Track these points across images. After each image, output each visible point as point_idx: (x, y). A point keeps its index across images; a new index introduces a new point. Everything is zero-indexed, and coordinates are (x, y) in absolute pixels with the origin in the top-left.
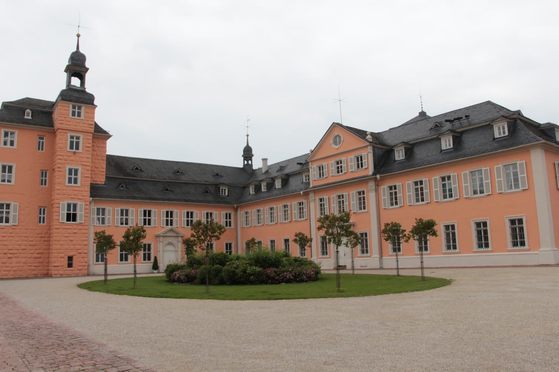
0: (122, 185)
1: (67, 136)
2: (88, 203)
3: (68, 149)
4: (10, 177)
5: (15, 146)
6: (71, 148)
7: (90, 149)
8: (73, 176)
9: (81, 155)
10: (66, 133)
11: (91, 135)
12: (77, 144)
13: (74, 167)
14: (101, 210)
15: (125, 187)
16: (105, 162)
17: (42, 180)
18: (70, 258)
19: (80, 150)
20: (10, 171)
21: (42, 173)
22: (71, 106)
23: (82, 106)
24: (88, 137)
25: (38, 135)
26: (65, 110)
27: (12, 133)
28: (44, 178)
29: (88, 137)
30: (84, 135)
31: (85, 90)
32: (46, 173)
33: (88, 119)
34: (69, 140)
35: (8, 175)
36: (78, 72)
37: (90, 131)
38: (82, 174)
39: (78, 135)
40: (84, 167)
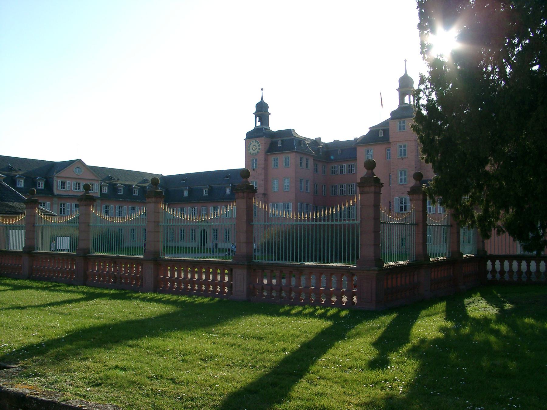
12: (405, 150)
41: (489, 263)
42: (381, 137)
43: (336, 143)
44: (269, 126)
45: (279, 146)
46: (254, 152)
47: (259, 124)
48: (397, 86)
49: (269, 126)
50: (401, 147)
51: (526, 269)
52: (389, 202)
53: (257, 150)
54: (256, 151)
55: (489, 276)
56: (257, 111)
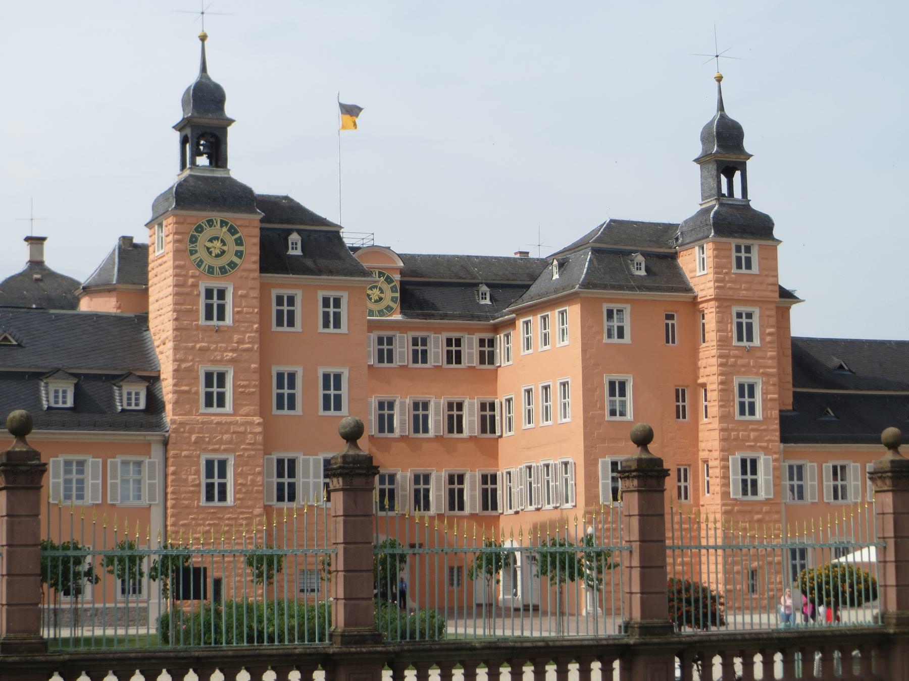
0: (828, 412)
1: (731, 313)
3: (735, 342)
4: (623, 404)
5: (627, 339)
6: (740, 339)
7: (775, 338)
9: (759, 354)
10: (728, 306)
11: (773, 306)
12: (750, 326)
13: (747, 380)
15: (832, 414)
16: (790, 360)
17: (678, 407)
18: (753, 573)
19: (757, 342)
20: (623, 393)
21: (677, 391)
23: (753, 245)
25: (665, 311)
27: (620, 311)
28: (681, 404)
30: (760, 307)
31: (749, 205)
32: (683, 391)
33: (766, 273)
34: (735, 320)
35: (620, 401)
36: (731, 166)
37: (768, 298)
38: (764, 393)
39: (749, 309)
42: (640, 276)
54: (223, 261)
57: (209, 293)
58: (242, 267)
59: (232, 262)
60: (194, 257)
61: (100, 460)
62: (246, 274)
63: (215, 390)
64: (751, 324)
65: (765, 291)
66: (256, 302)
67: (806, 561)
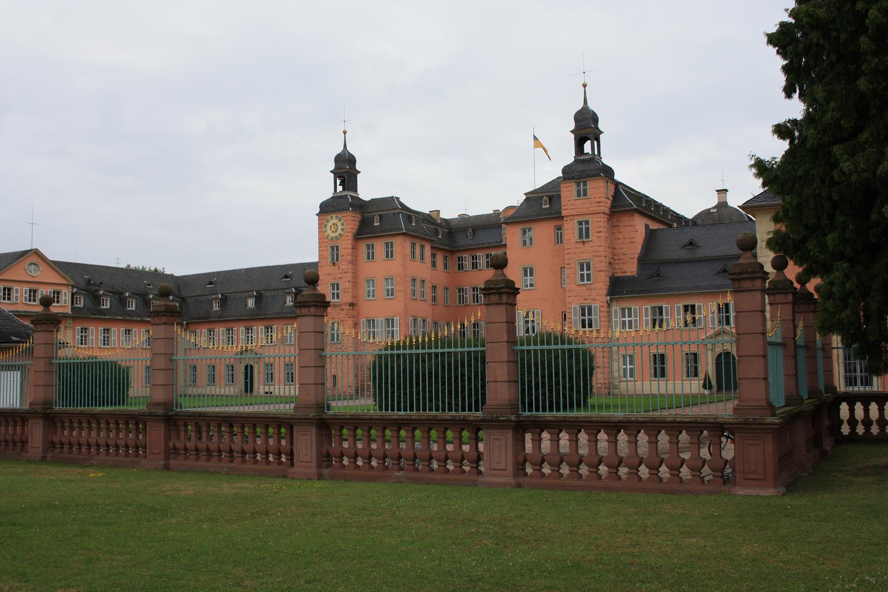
2: (605, 304)
6: (581, 236)
8: (585, 272)
12: (587, 229)
14: (626, 310)
20: (531, 275)
22: (574, 186)
24: (599, 219)
25: (555, 226)
26: (567, 191)
29: (599, 219)
33: (595, 196)
36: (584, 136)
40: (596, 259)
41: (844, 408)
42: (546, 208)
43: (463, 218)
44: (357, 192)
45: (375, 224)
46: (333, 235)
47: (340, 188)
48: (572, 126)
49: (358, 193)
50: (580, 223)
51: (849, 416)
52: (562, 312)
53: (339, 231)
54: (337, 234)
55: (845, 430)
56: (336, 168)
57: (333, 248)
58: (345, 235)
59: (340, 234)
60: (325, 234)
61: (256, 327)
62: (345, 238)
63: (336, 291)
64: (588, 227)
65: (594, 207)
66: (350, 251)
67: (698, 365)
